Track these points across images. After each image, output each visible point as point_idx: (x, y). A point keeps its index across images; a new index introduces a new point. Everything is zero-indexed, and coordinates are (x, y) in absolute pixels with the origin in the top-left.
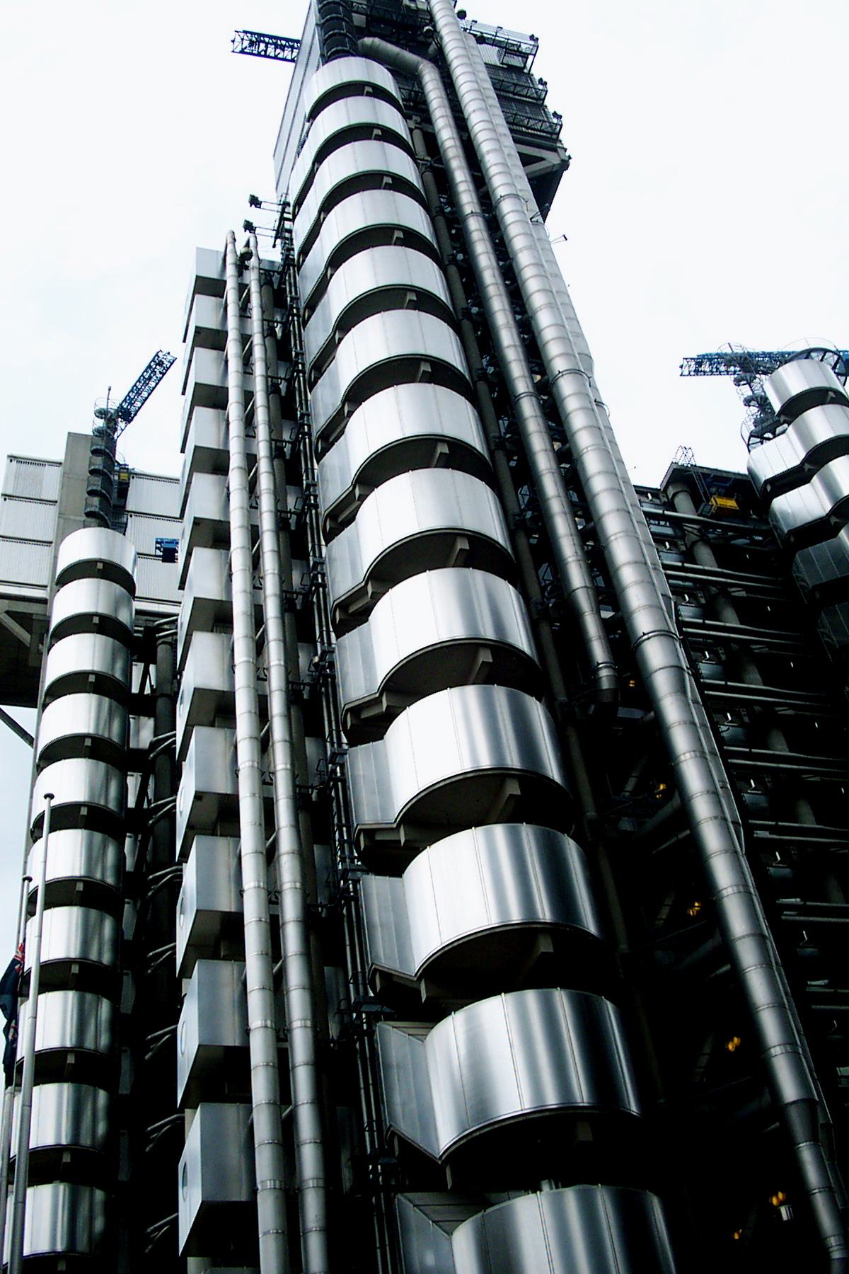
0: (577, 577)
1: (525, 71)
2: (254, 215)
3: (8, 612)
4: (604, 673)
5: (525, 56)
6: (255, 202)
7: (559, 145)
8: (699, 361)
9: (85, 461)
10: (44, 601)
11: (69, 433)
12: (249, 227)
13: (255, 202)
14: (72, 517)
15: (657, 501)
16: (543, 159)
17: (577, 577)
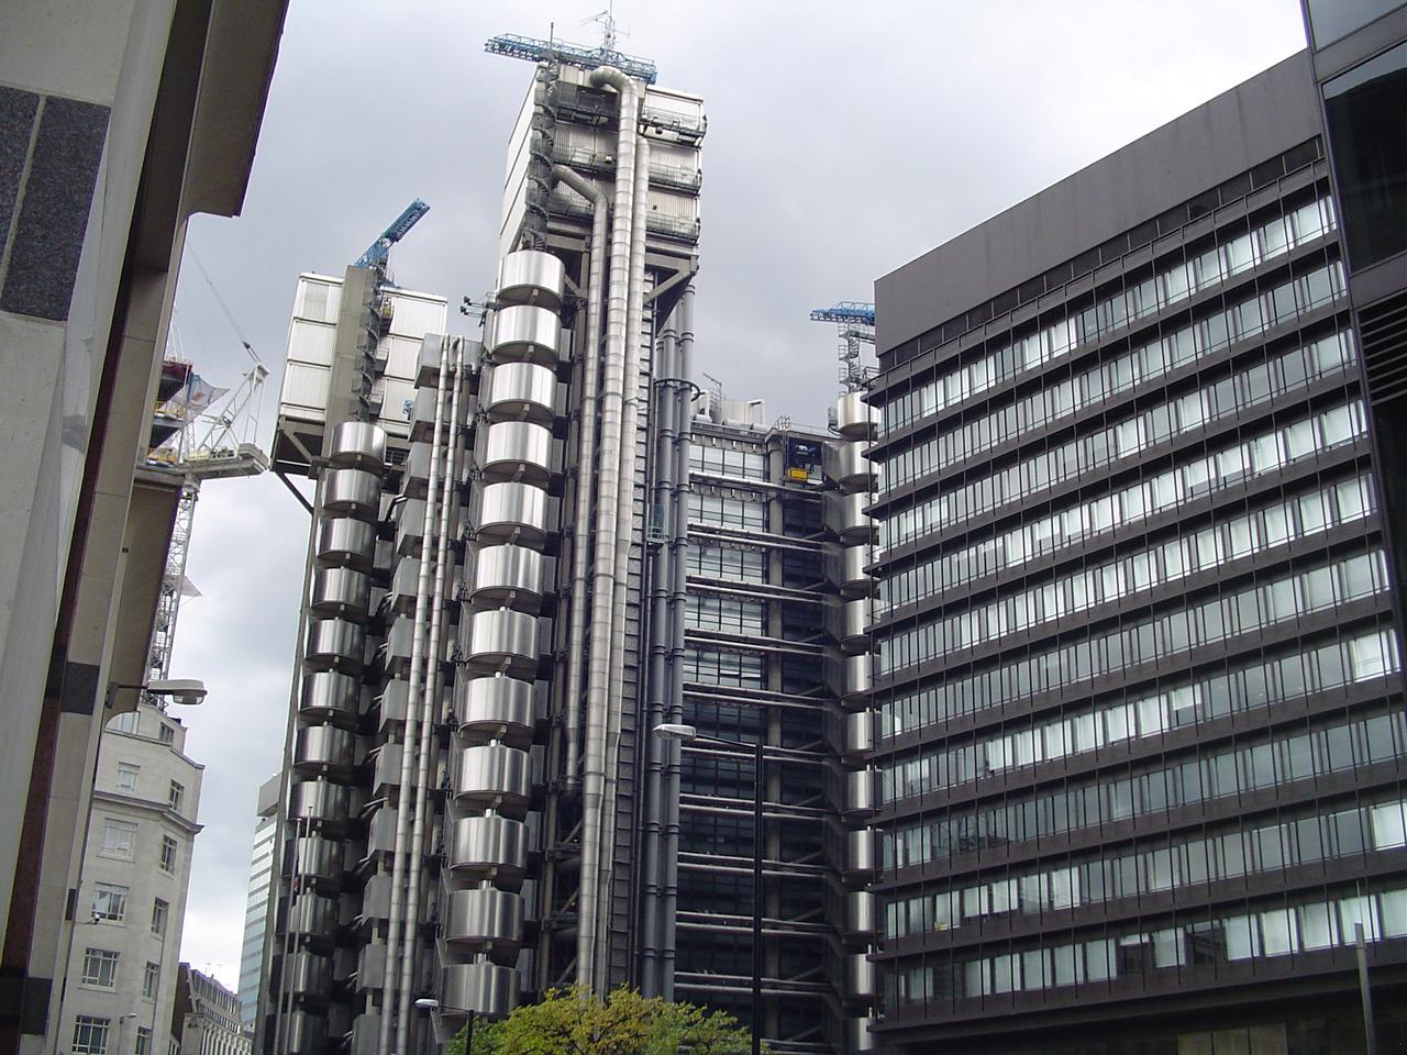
0: (572, 722)
1: (696, 144)
2: (466, 305)
3: (295, 434)
4: (570, 781)
5: (697, 137)
6: (467, 300)
7: (695, 252)
8: (827, 315)
9: (359, 307)
10: (322, 424)
11: (349, 266)
12: (463, 310)
13: (467, 300)
14: (346, 356)
15: (759, 450)
16: (676, 272)
17: (572, 722)
